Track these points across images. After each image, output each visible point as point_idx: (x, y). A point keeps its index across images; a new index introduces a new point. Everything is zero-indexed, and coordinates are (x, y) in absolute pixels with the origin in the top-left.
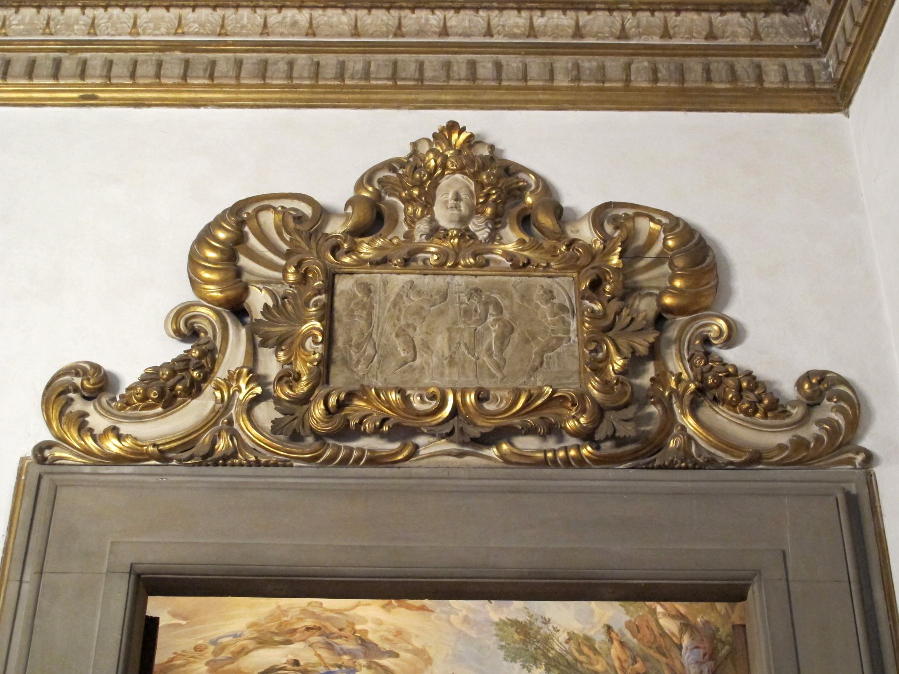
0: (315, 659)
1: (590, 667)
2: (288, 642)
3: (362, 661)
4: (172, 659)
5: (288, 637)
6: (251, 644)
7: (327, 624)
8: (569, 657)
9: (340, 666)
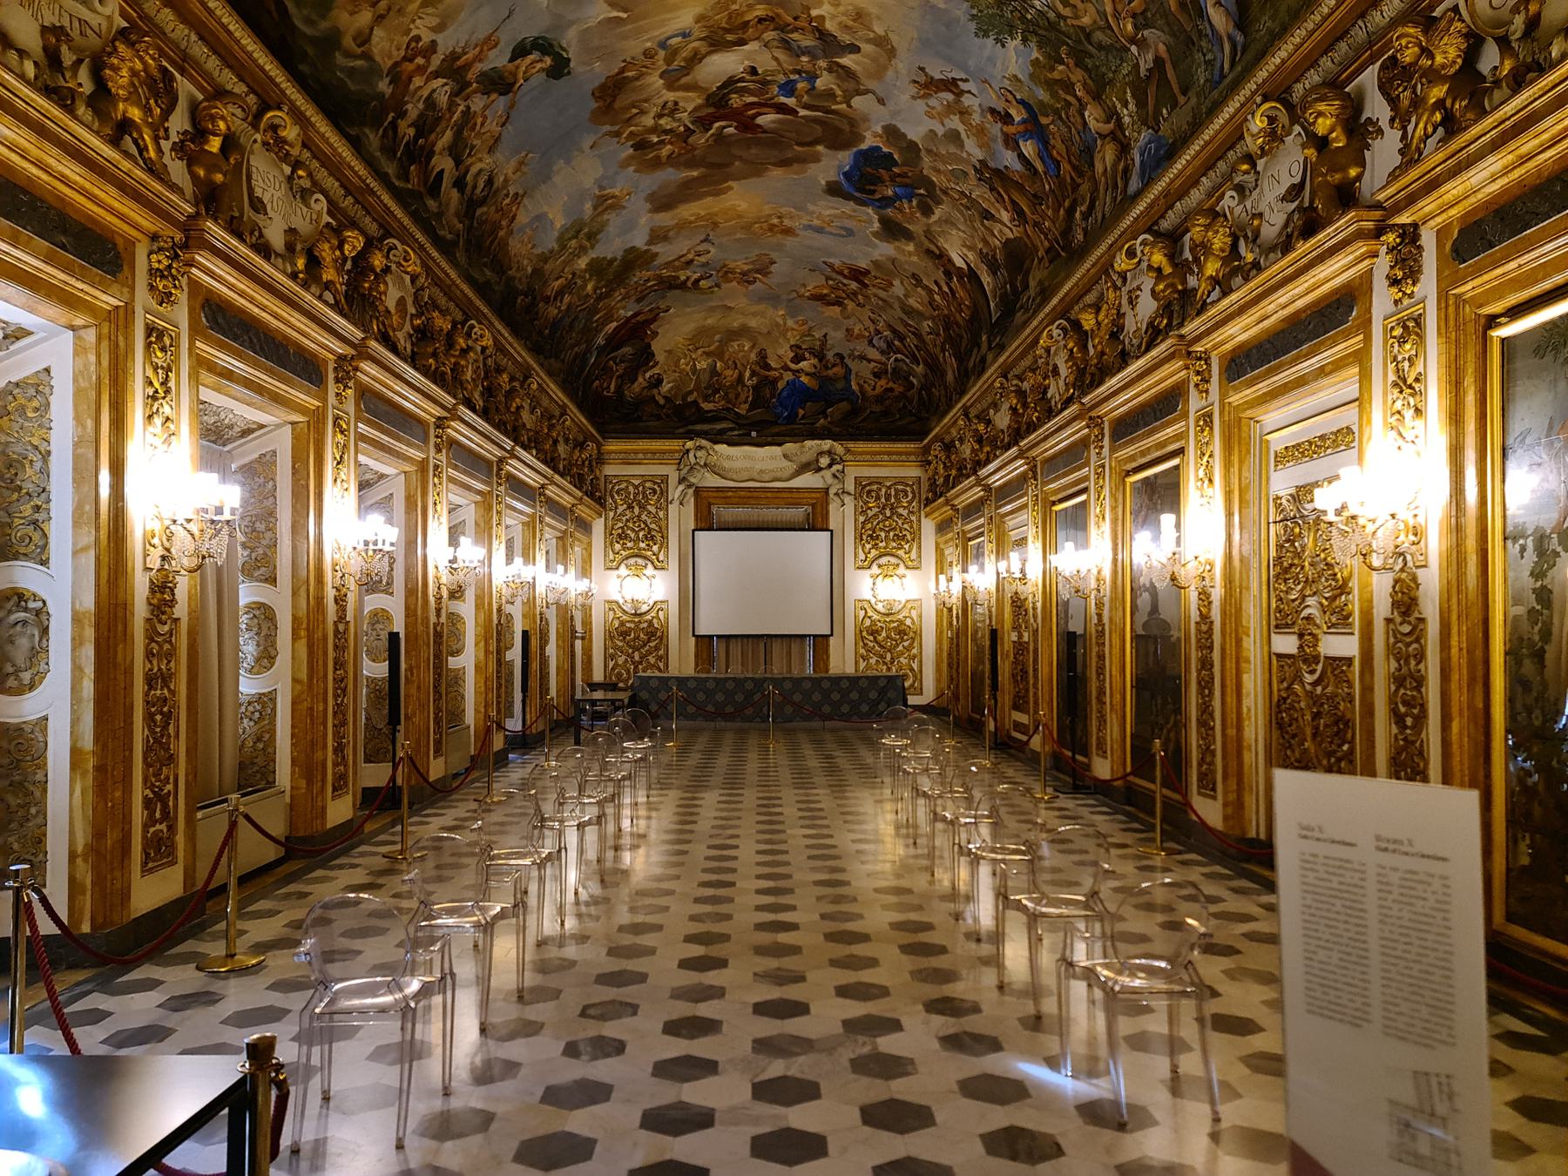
0: (773, 65)
1: (1075, 22)
2: (742, 42)
3: (822, 63)
4: (622, 71)
7: (780, 11)
8: (1051, 15)
9: (799, 72)
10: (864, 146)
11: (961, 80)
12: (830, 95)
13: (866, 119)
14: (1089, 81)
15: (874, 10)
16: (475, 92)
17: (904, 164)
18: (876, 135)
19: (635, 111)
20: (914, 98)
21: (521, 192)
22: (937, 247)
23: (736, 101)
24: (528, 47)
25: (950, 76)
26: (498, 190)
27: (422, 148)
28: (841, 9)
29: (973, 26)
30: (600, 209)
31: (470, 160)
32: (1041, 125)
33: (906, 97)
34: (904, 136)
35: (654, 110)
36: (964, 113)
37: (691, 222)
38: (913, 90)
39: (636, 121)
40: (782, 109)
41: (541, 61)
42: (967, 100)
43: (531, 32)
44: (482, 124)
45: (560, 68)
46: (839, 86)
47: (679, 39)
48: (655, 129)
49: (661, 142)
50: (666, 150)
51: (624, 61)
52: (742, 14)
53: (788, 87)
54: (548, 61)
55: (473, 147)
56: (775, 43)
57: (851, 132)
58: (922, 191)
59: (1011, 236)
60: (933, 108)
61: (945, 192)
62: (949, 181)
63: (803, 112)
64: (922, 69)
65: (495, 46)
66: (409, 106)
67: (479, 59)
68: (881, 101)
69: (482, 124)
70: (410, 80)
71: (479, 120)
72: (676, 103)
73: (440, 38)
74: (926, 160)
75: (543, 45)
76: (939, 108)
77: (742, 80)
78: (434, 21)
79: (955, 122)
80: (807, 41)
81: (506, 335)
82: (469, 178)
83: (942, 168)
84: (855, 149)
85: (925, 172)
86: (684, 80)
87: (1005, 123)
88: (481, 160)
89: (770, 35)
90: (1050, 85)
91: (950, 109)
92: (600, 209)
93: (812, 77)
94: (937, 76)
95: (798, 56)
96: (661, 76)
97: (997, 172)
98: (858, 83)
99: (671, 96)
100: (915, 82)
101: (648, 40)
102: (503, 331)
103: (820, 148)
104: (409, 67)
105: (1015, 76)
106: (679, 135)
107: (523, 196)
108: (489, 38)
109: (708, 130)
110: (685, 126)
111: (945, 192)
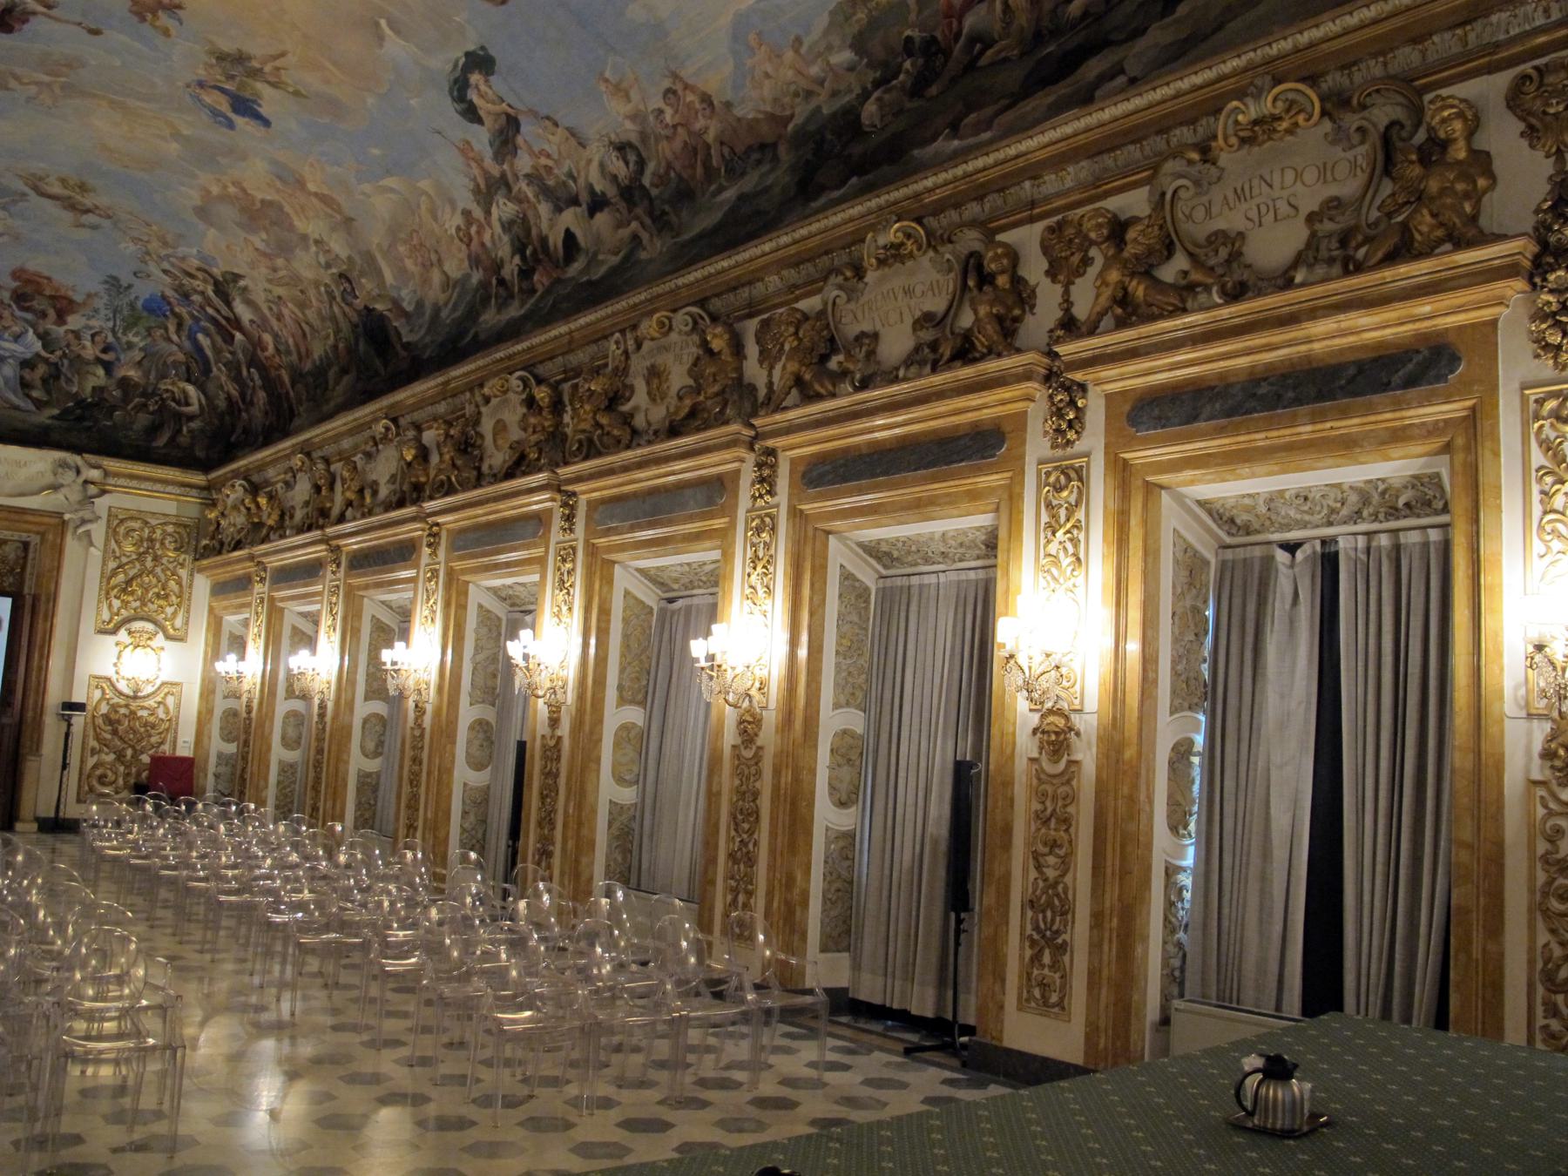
16: (512, 165)
21: (667, 84)
24: (464, 106)
26: (644, 136)
27: (535, 252)
31: (581, 181)
41: (477, 87)
43: (449, 109)
44: (548, 156)
45: (480, 62)
54: (475, 78)
55: (570, 175)
65: (468, 143)
66: (500, 254)
67: (479, 161)
69: (548, 156)
70: (483, 245)
71: (543, 161)
73: (461, 205)
75: (459, 90)
78: (448, 209)
81: (725, 264)
82: (598, 188)
88: (589, 161)
102: (711, 269)
104: (475, 243)
107: (675, 76)
108: (462, 151)
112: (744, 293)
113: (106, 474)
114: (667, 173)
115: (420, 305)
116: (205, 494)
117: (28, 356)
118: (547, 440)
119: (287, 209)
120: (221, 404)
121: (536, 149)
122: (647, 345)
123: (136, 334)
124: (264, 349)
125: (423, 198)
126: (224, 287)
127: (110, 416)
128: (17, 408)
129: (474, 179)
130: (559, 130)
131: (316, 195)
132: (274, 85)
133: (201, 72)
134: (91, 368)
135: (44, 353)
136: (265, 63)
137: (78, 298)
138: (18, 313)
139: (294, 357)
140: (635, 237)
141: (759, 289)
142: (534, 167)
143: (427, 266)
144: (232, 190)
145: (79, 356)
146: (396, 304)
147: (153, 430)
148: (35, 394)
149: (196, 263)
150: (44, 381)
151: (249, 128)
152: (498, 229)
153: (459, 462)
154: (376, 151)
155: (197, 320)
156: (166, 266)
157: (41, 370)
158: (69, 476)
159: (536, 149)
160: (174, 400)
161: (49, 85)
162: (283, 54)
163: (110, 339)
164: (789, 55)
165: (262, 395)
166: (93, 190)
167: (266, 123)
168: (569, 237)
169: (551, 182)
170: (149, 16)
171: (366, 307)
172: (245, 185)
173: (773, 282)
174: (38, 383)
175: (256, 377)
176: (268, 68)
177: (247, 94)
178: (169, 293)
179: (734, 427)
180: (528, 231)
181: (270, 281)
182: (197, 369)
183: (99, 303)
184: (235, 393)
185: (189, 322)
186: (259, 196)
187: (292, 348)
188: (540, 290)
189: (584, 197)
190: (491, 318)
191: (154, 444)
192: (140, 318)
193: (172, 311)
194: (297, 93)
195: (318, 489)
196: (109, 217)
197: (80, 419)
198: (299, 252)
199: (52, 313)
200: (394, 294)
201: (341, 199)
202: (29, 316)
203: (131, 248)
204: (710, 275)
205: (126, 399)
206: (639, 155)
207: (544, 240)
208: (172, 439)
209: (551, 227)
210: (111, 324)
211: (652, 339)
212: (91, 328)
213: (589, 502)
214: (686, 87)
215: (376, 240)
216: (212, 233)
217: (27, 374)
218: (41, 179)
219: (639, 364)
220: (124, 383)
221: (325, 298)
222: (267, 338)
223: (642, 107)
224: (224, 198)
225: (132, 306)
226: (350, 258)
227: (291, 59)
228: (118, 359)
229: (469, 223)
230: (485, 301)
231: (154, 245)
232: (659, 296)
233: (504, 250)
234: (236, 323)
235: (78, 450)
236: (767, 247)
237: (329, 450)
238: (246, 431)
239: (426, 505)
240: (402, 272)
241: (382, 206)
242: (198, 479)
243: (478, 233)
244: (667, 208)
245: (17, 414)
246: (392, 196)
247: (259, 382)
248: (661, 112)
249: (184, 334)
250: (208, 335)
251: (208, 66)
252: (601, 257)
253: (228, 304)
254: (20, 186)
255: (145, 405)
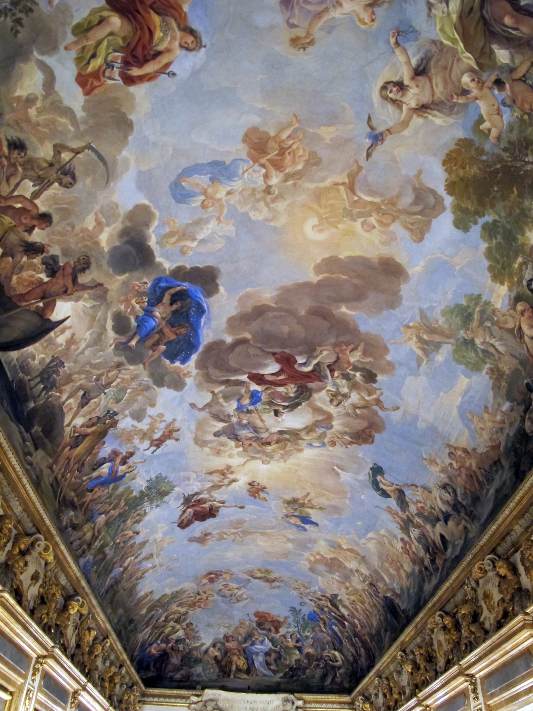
0: (265, 416)
2: (281, 432)
4: (351, 443)
5: (281, 437)
6: (303, 434)
7: (259, 448)
8: (139, 507)
9: (248, 412)
10: (194, 357)
11: (155, 451)
12: (227, 398)
13: (199, 386)
14: (113, 518)
15: (212, 457)
17: (159, 359)
18: (188, 374)
19: (358, 411)
20: (175, 420)
21: (447, 451)
22: (84, 287)
23: (291, 390)
24: (381, 492)
25: (162, 447)
26: (450, 478)
28: (227, 454)
29: (164, 475)
30: (437, 338)
31: (437, 509)
32: (110, 483)
33: (179, 418)
34: (169, 387)
35: (347, 403)
36: (144, 435)
37: (377, 208)
38: (177, 425)
39: (362, 403)
40: (259, 379)
42: (147, 443)
43: (376, 495)
45: (377, 470)
46: (222, 406)
47: (314, 444)
48: (354, 386)
49: (355, 369)
50: (355, 357)
51: (347, 447)
52: (279, 448)
53: (255, 397)
54: (379, 478)
56: (261, 431)
57: (207, 368)
58: (133, 343)
59: (67, 421)
60: (161, 422)
61: (119, 365)
62: (123, 379)
63: (244, 378)
64: (177, 440)
68: (193, 406)
69: (420, 502)
70: (414, 552)
71: (420, 505)
72: (331, 401)
74: (146, 378)
75: (376, 485)
76: (158, 425)
77: (285, 407)
78: (395, 541)
79: (144, 425)
80: (244, 433)
81: (494, 527)
83: (134, 384)
84: (201, 349)
85: (141, 366)
86: (320, 418)
87: (123, 459)
88: (436, 499)
89: (265, 435)
90: (120, 497)
91: (152, 429)
92: (437, 338)
93: (239, 409)
94: (169, 442)
95: (249, 423)
96: (331, 427)
97: (103, 434)
98: (210, 413)
99: (332, 409)
100: (178, 430)
101: (330, 451)
103: (229, 339)
104: (411, 553)
105: (134, 479)
106: (340, 369)
107: (449, 446)
109: (318, 364)
110: (332, 376)
111: (119, 365)
112: (508, 539)
113: (305, 702)
114: (466, 492)
115: (402, 589)
116: (351, 706)
117: (267, 650)
118: (455, 647)
119: (340, 559)
120: (351, 658)
121: (415, 501)
122: (481, 582)
123: (309, 631)
124: (357, 627)
125: (385, 538)
126: (333, 600)
127: (304, 673)
128: (265, 675)
129: (399, 523)
130: (419, 489)
131: (347, 550)
132: (312, 507)
133: (285, 511)
134: (293, 651)
135: (273, 648)
136: (304, 500)
137: (281, 620)
138: (260, 631)
139: (368, 628)
140: (465, 528)
141: (514, 536)
142: (417, 509)
143: (398, 569)
144: (318, 557)
145: (287, 647)
146: (393, 590)
147: (324, 677)
148: (272, 667)
149: (319, 593)
150: (275, 661)
151: (311, 529)
152: (416, 543)
153: (428, 668)
154: (359, 523)
155: (330, 619)
156: (310, 598)
157: (273, 655)
158: (289, 706)
159: (415, 501)
160: (330, 660)
161: (237, 533)
162: (308, 494)
163: (298, 636)
164: (486, 416)
165: (362, 650)
166: (272, 572)
167: (316, 524)
168: (442, 536)
169: (426, 514)
170: (257, 495)
171: (384, 597)
172: (322, 553)
173: (518, 529)
174: (273, 662)
175: (358, 642)
176: (306, 502)
177: (304, 515)
178: (316, 609)
179: (520, 617)
180: (427, 541)
181: (348, 594)
182: (337, 645)
183: (290, 620)
184: (354, 652)
185: (327, 621)
186: (328, 557)
187: (366, 624)
188: (440, 567)
189: (441, 516)
190: (428, 587)
191: (326, 684)
192: (308, 624)
193: (320, 618)
194: (321, 508)
195: (385, 695)
196: (282, 581)
197: (292, 676)
198: (353, 578)
199: (273, 629)
200: (391, 587)
201: (356, 548)
202: (264, 632)
203: (295, 593)
204: (492, 536)
205: (310, 664)
206: (452, 488)
207: (434, 542)
208: (333, 680)
209: (434, 534)
210: (297, 629)
211: (481, 578)
212: (288, 632)
213: (481, 679)
214: (456, 448)
215: (376, 564)
216: (319, 578)
217: (268, 658)
218: (252, 572)
219: (480, 593)
220: (308, 655)
221: (369, 596)
222: (356, 621)
223: (444, 465)
224: (317, 561)
225: (303, 619)
226: (370, 574)
227: (312, 495)
228: (303, 645)
229: (405, 545)
230: (423, 580)
231: (302, 589)
232: (476, 554)
233: (422, 553)
234: (343, 616)
235: (291, 692)
236: (507, 512)
237: (387, 672)
238: (362, 670)
239: (419, 695)
240: (390, 575)
241: (372, 546)
242: (346, 699)
243: (410, 547)
244: (472, 508)
245: (265, 678)
246: (373, 541)
247: (360, 644)
248: (451, 464)
249: (328, 627)
250: (336, 626)
251: (286, 508)
252: (456, 543)
253: (338, 609)
254: (246, 577)
255: (318, 665)
